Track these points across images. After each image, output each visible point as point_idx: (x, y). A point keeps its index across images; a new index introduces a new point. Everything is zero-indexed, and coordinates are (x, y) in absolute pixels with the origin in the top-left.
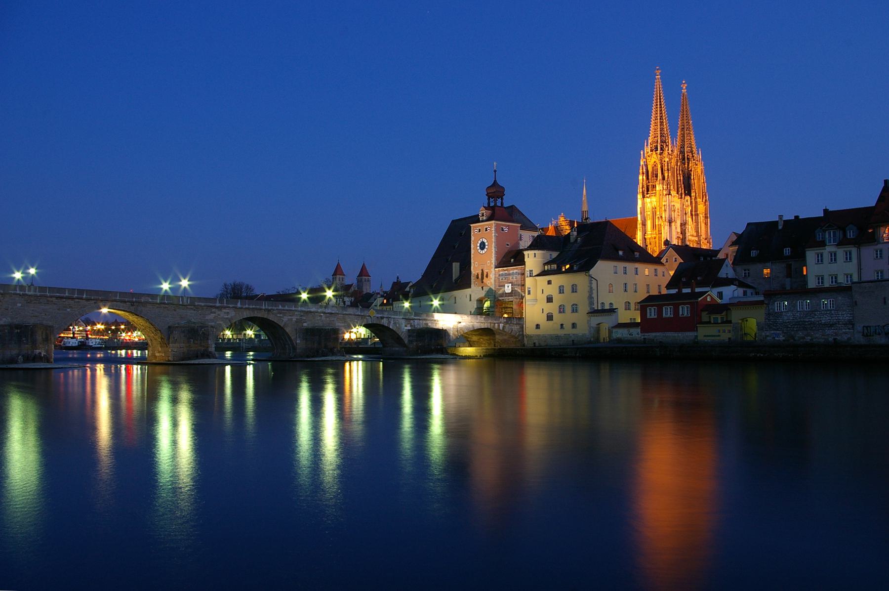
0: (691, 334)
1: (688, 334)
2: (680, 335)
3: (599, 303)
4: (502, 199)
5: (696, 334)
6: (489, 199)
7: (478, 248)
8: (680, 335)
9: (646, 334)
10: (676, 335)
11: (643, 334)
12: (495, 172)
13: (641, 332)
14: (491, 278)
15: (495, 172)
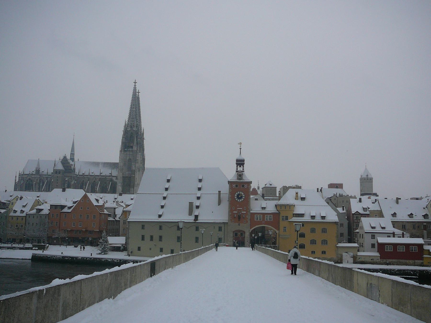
0: (418, 261)
1: (418, 261)
2: (410, 261)
3: (359, 242)
4: (243, 167)
5: (422, 262)
6: (237, 167)
7: (236, 197)
8: (410, 261)
9: (384, 260)
10: (407, 261)
11: (382, 260)
12: (240, 150)
13: (380, 259)
14: (247, 219)
15: (240, 150)
